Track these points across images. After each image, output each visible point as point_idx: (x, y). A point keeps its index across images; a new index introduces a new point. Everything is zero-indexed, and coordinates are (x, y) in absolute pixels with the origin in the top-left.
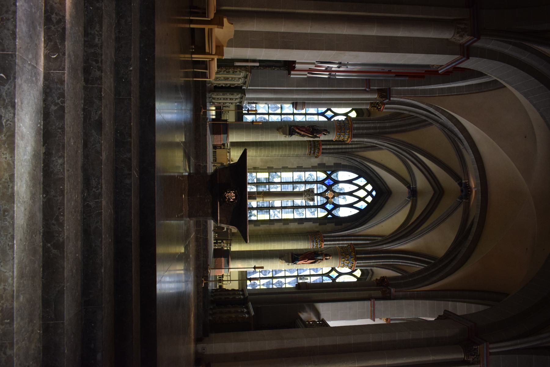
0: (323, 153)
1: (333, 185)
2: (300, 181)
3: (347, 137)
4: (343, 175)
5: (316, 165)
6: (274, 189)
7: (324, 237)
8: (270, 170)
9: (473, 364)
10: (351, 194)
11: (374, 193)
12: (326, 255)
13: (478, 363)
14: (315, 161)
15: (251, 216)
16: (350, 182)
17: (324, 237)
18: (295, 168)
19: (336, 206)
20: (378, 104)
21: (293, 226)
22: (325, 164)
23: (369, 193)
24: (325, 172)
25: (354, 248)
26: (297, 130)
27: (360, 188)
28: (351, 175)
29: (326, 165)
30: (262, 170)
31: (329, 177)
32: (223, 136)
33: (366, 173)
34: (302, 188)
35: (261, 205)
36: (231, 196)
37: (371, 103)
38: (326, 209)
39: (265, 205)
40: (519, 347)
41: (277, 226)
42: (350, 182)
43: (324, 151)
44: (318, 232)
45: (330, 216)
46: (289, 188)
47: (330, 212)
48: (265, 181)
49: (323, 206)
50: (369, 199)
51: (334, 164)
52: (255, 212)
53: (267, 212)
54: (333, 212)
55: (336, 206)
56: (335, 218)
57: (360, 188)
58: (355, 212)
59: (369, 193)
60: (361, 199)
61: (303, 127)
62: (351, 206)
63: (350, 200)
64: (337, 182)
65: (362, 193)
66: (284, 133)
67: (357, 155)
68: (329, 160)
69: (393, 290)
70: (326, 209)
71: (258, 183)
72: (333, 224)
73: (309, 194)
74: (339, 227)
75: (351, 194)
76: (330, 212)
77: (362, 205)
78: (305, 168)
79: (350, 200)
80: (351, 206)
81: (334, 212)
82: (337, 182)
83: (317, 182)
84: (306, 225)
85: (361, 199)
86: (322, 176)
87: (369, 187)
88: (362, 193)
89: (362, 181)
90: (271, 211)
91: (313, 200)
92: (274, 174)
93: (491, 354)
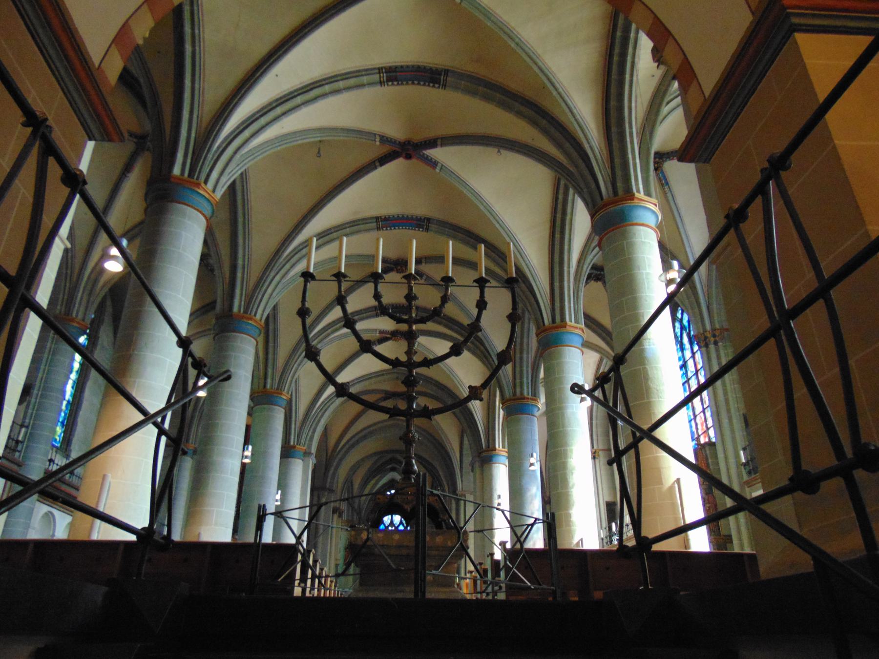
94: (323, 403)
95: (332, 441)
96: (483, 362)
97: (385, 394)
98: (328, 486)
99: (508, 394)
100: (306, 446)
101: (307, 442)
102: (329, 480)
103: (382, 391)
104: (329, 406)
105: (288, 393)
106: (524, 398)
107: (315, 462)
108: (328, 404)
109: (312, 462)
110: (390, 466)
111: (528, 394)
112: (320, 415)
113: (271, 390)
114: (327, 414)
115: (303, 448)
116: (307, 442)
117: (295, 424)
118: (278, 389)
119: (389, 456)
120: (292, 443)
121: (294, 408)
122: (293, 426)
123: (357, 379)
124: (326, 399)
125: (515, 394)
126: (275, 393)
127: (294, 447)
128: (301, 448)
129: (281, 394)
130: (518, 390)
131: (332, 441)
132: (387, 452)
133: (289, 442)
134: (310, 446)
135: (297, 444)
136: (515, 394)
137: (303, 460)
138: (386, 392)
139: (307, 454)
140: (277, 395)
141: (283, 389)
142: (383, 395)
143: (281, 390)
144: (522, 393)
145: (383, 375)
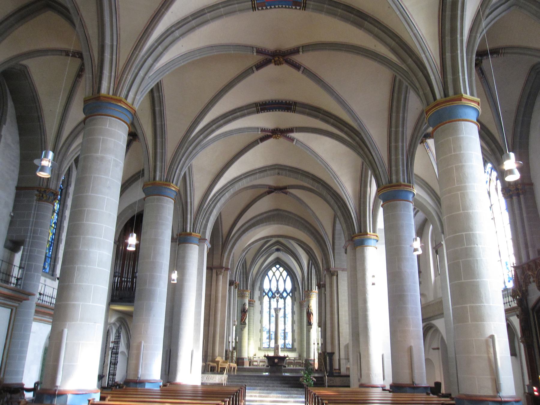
0: (253, 299)
1: (272, 292)
2: (269, 313)
3: (247, 293)
4: (266, 286)
5: (259, 302)
6: (273, 329)
7: (303, 299)
8: (261, 331)
9: (338, 273)
10: (277, 281)
11: (278, 266)
12: (309, 307)
13: (337, 271)
14: (257, 303)
15: (289, 344)
16: (270, 281)
17: (303, 299)
18: (261, 315)
19: (285, 290)
20: (235, 285)
21: (296, 317)
22: (259, 297)
23: (278, 269)
24: (264, 296)
25: (306, 291)
26: (244, 320)
27: (274, 275)
28: (266, 280)
29: (259, 295)
30: (261, 336)
31: (267, 294)
32: (245, 360)
33: (265, 272)
34: (273, 312)
35: (283, 338)
36: (276, 361)
37: (235, 288)
38: (287, 296)
39: (283, 335)
40: (332, 256)
41: (296, 328)
42: (270, 281)
43: (252, 298)
44: (300, 302)
45: (291, 294)
46: (273, 319)
47: (288, 294)
48: (268, 334)
49: (285, 299)
50: (281, 269)
51: (259, 291)
52: (287, 342)
53: (287, 334)
54: (288, 292)
55: (285, 290)
56: (291, 291)
57: (274, 275)
58: (289, 279)
59: (278, 269)
60: (281, 275)
61: (242, 317)
62: (285, 281)
63: (281, 281)
64: (270, 290)
65: (278, 274)
66: (245, 327)
67: (255, 277)
68: (257, 294)
69: (321, 283)
70: (287, 296)
71: (269, 338)
72: (296, 293)
73: (277, 310)
74: (297, 288)
75: (277, 281)
76: (288, 294)
77: (285, 274)
78: (261, 309)
79: (281, 281)
80: (285, 281)
81: (288, 292)
82: (270, 290)
83: (270, 302)
84: (296, 309)
85: (281, 275)
86: (266, 299)
87: (274, 269)
88: (278, 274)
89: (270, 273)
90: (286, 331)
91: (280, 309)
92: (264, 328)
93: (335, 267)
94: (215, 195)
95: (225, 228)
96: (359, 153)
97: (269, 188)
98: (224, 266)
99: (384, 181)
101: (202, 230)
102: (225, 260)
103: (267, 185)
104: (220, 198)
105: (177, 185)
106: (400, 185)
108: (219, 197)
109: (207, 246)
110: (275, 248)
111: (404, 181)
112: (213, 205)
113: (160, 182)
114: (219, 205)
115: (198, 235)
116: (202, 230)
118: (166, 181)
119: (274, 240)
120: (188, 231)
121: (189, 200)
122: (189, 216)
124: (217, 192)
125: (390, 181)
126: (164, 184)
127: (190, 234)
129: (169, 185)
130: (394, 177)
131: (225, 228)
132: (272, 237)
133: (186, 231)
134: (204, 233)
135: (193, 231)
136: (390, 181)
137: (198, 246)
138: (270, 187)
139: (202, 240)
140: (165, 186)
142: (267, 189)
143: (169, 182)
144: (398, 181)
145: (266, 171)
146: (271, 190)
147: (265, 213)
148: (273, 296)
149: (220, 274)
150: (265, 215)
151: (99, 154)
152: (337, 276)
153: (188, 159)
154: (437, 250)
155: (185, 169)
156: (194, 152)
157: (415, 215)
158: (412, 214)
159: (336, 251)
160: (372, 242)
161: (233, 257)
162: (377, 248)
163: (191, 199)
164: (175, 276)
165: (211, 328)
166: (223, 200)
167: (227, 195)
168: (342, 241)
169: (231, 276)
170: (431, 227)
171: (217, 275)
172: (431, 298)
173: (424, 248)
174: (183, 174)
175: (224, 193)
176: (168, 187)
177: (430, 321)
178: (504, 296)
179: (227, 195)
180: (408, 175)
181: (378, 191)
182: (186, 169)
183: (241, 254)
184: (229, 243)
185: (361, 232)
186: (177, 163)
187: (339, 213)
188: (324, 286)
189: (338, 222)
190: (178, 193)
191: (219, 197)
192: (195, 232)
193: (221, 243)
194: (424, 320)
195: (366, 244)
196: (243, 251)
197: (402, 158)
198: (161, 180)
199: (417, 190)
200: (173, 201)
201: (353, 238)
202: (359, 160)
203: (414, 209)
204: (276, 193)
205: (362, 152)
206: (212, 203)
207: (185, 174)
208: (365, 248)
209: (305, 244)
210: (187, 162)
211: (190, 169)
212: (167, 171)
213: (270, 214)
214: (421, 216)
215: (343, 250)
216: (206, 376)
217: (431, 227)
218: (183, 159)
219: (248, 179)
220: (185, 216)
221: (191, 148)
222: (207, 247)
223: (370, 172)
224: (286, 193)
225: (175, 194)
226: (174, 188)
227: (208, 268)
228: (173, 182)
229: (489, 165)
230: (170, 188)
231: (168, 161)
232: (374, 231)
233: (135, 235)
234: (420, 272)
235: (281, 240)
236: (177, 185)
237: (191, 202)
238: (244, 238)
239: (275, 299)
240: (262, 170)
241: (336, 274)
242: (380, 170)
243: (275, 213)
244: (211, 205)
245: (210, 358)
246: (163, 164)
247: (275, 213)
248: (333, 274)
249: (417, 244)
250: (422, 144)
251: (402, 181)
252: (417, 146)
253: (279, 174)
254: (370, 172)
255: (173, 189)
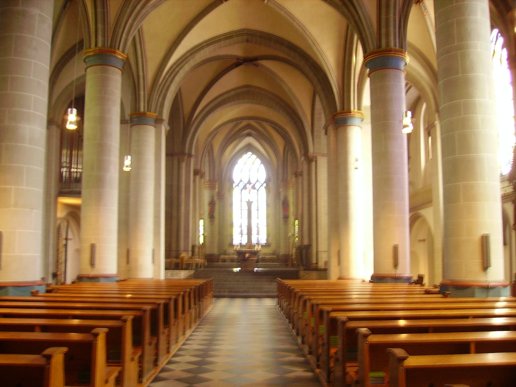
94: (172, 67)
95: (187, 107)
96: (343, 13)
97: (237, 59)
98: (187, 151)
99: (371, 47)
100: (157, 112)
101: (158, 109)
103: (235, 56)
105: (123, 52)
106: (391, 50)
107: (168, 128)
108: (177, 70)
109: (164, 128)
110: (246, 132)
111: (395, 46)
112: (170, 79)
114: (177, 79)
116: (158, 109)
117: (144, 91)
118: (111, 47)
119: (244, 123)
120: (142, 110)
121: (141, 74)
122: (142, 93)
123: (206, 42)
124: (174, 64)
127: (144, 114)
128: (153, 114)
129: (115, 52)
131: (187, 107)
132: (242, 119)
133: (139, 110)
134: (161, 112)
135: (148, 111)
138: (238, 58)
139: (158, 121)
141: (117, 47)
143: (115, 48)
146: (238, 63)
147: (233, 90)
148: (245, 187)
149: (183, 161)
150: (233, 93)
151: (20, 8)
152: (316, 161)
153: (137, 21)
154: (429, 131)
155: (134, 32)
156: (144, 11)
157: (407, 91)
158: (404, 90)
159: (315, 134)
160: (356, 121)
161: (197, 141)
162: (361, 128)
163: (143, 72)
164: (128, 161)
165: (174, 222)
166: (182, 74)
167: (187, 68)
168: (321, 120)
169: (196, 164)
170: (424, 106)
171: (179, 162)
172: (420, 185)
173: (416, 125)
174: (130, 39)
175: (183, 64)
176: (113, 54)
177: (418, 210)
178: (502, 181)
179: (187, 68)
180: (400, 38)
181: (365, 57)
182: (134, 33)
183: (206, 140)
184: (192, 125)
185: (343, 109)
186: (123, 24)
187: (319, 88)
188: (301, 174)
189: (317, 99)
190: (126, 63)
191: (177, 70)
192: (150, 111)
193: (182, 126)
194: (411, 210)
195: (349, 122)
196: (209, 135)
197: (394, 17)
198: (104, 47)
199: (408, 58)
200: (120, 72)
201: (335, 115)
202: (345, 22)
203: (407, 85)
204: (246, 65)
205: (346, 11)
206: (169, 76)
207: (134, 39)
208: (349, 127)
209: (280, 127)
210: (135, 23)
211: (140, 32)
212: (110, 35)
213: (238, 91)
214: (414, 93)
215: (323, 132)
216: (170, 272)
217: (424, 106)
218: (130, 21)
219: (211, 47)
220: (137, 93)
221: (139, 7)
222: (166, 128)
223: (356, 37)
224: (257, 66)
225: (122, 63)
226: (120, 55)
227: (168, 155)
228: (118, 49)
229: (496, 31)
230: (116, 55)
231: (112, 23)
232: (359, 108)
233: (75, 111)
234: (409, 158)
235: (253, 123)
236: (123, 52)
237: (144, 76)
238: (209, 119)
239: (247, 190)
240: (228, 37)
241: (315, 160)
242: (367, 32)
243: (245, 89)
244: (168, 78)
245: (174, 254)
246: (106, 26)
247: (245, 89)
248: (310, 160)
249: (407, 120)
250: (418, 3)
251: (392, 44)
252: (411, 7)
253: (247, 41)
254: (356, 37)
255: (120, 57)
